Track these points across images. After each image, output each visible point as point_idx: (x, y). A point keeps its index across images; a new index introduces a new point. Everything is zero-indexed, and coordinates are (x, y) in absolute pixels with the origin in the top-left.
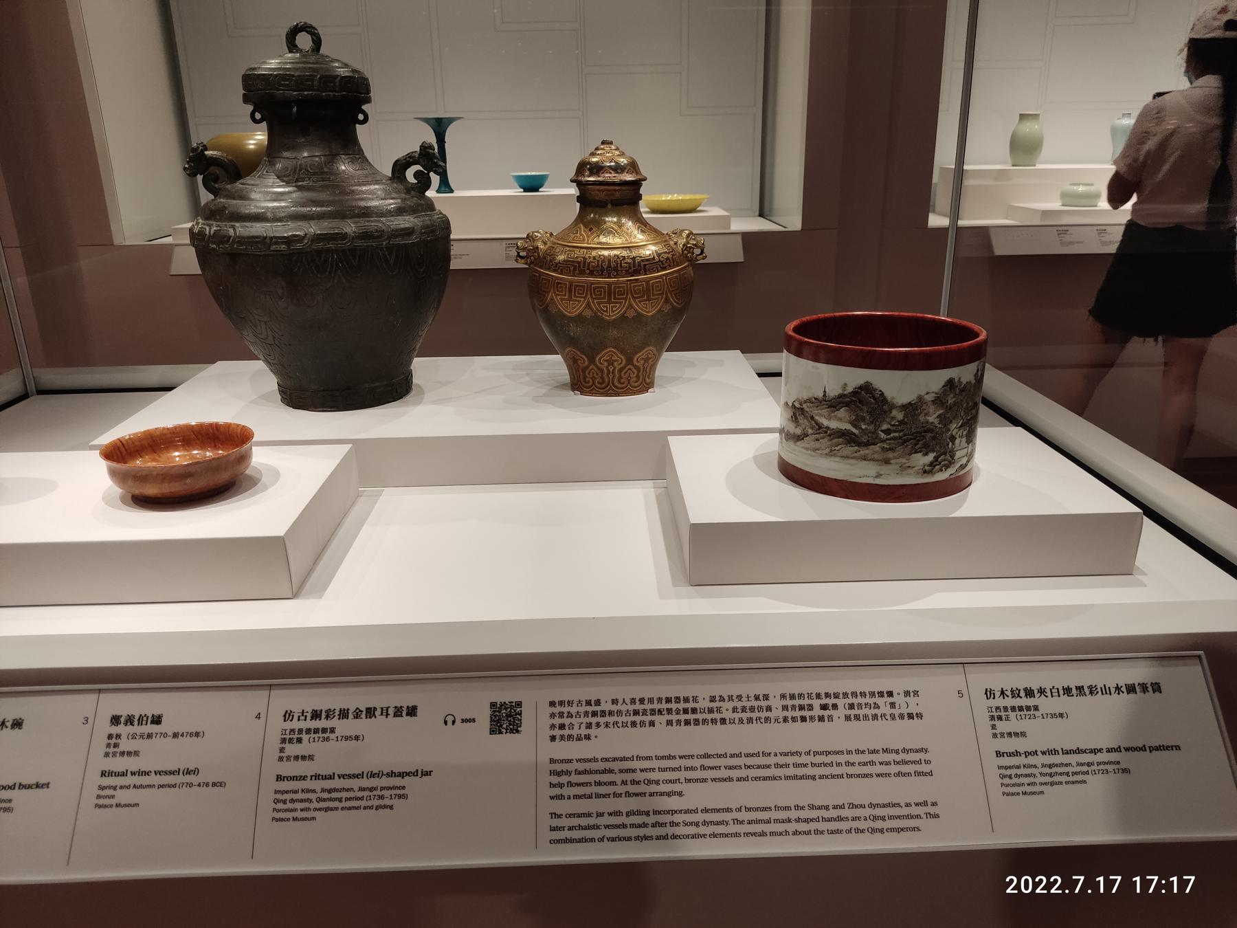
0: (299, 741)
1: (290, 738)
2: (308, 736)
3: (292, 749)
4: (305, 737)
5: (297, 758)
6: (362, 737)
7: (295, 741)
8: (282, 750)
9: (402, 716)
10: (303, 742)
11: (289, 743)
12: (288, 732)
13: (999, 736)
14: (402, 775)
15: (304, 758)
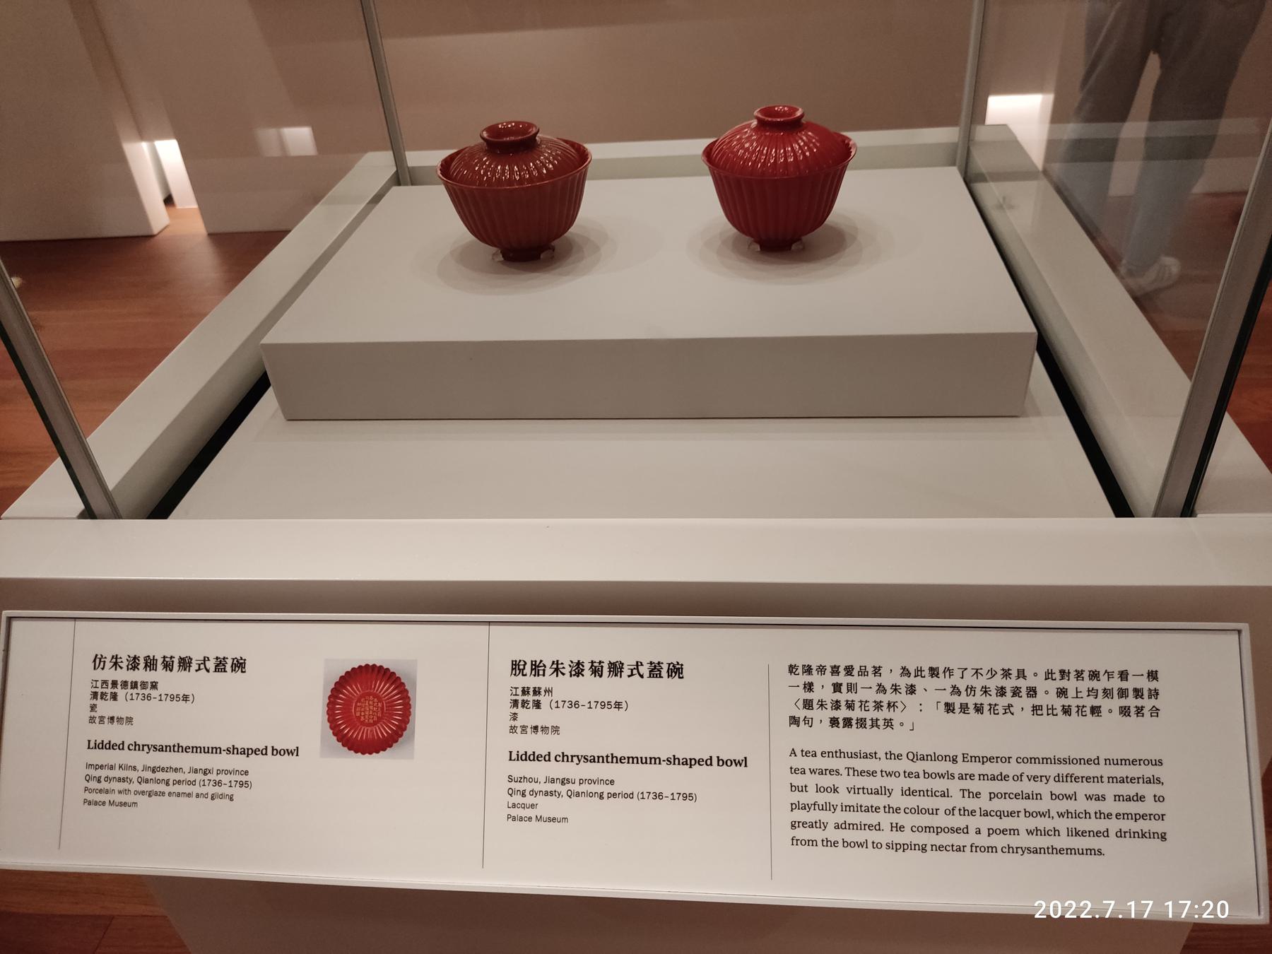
0: (114, 697)
1: (102, 693)
2: (124, 691)
3: (106, 708)
4: (120, 692)
5: (112, 718)
6: (191, 696)
7: (108, 697)
8: (93, 708)
9: (225, 671)
10: (118, 698)
11: (102, 698)
12: (99, 684)
13: (519, 730)
14: (246, 752)
15: (120, 720)
